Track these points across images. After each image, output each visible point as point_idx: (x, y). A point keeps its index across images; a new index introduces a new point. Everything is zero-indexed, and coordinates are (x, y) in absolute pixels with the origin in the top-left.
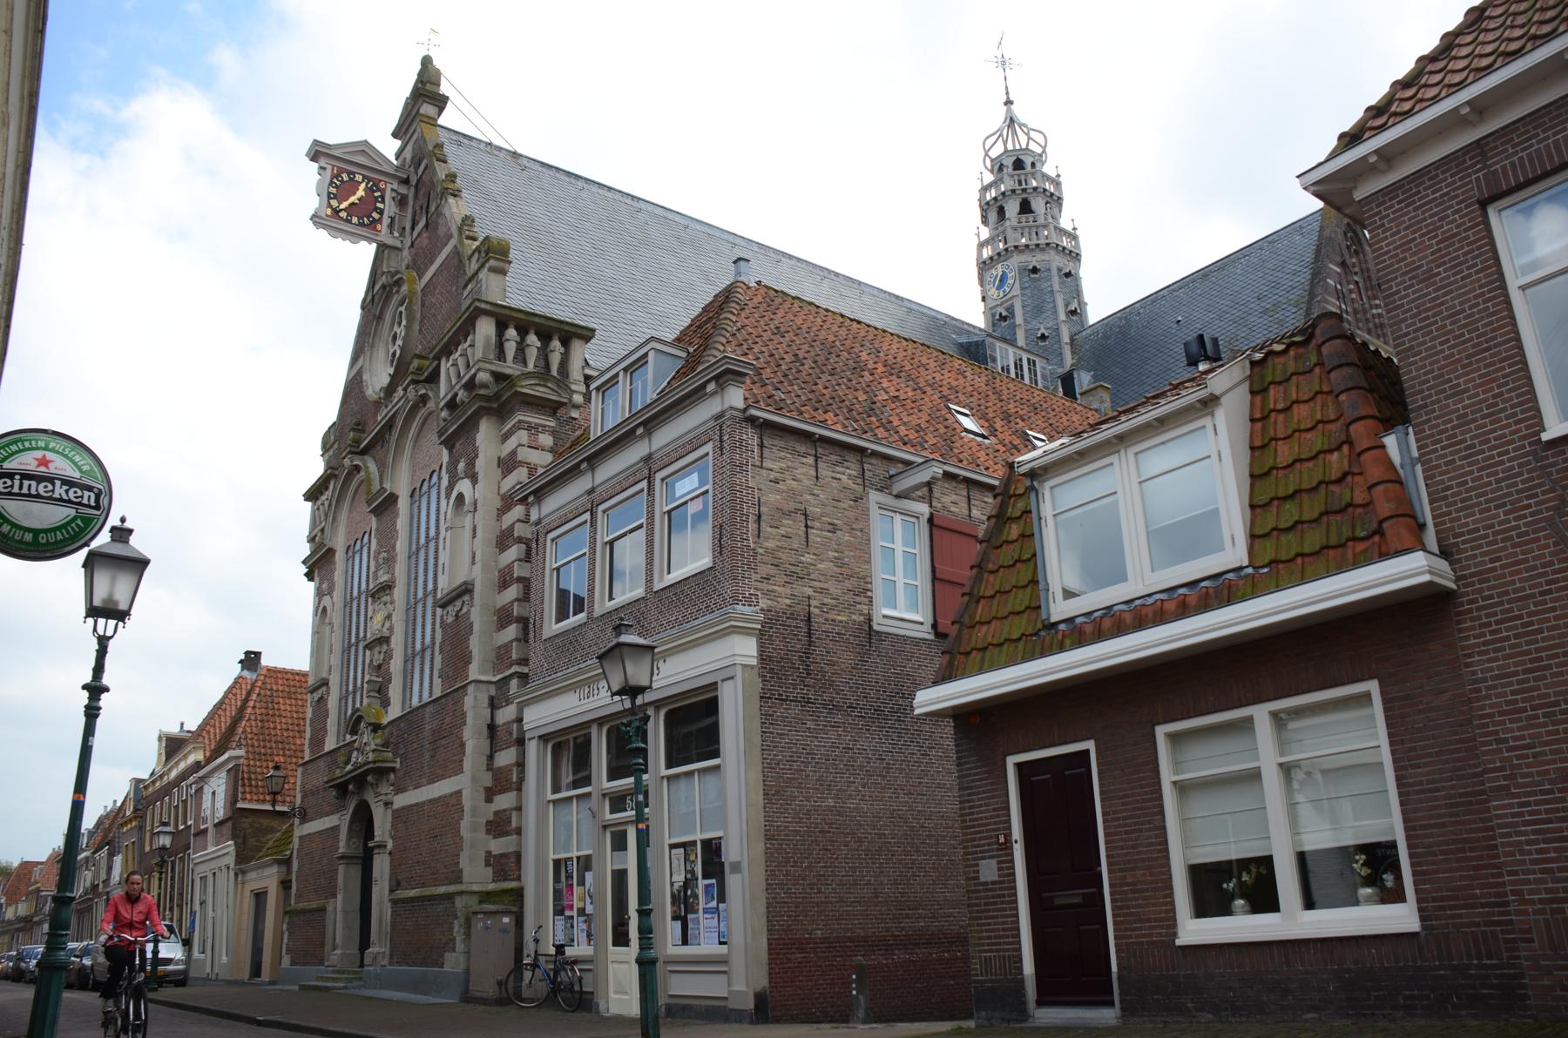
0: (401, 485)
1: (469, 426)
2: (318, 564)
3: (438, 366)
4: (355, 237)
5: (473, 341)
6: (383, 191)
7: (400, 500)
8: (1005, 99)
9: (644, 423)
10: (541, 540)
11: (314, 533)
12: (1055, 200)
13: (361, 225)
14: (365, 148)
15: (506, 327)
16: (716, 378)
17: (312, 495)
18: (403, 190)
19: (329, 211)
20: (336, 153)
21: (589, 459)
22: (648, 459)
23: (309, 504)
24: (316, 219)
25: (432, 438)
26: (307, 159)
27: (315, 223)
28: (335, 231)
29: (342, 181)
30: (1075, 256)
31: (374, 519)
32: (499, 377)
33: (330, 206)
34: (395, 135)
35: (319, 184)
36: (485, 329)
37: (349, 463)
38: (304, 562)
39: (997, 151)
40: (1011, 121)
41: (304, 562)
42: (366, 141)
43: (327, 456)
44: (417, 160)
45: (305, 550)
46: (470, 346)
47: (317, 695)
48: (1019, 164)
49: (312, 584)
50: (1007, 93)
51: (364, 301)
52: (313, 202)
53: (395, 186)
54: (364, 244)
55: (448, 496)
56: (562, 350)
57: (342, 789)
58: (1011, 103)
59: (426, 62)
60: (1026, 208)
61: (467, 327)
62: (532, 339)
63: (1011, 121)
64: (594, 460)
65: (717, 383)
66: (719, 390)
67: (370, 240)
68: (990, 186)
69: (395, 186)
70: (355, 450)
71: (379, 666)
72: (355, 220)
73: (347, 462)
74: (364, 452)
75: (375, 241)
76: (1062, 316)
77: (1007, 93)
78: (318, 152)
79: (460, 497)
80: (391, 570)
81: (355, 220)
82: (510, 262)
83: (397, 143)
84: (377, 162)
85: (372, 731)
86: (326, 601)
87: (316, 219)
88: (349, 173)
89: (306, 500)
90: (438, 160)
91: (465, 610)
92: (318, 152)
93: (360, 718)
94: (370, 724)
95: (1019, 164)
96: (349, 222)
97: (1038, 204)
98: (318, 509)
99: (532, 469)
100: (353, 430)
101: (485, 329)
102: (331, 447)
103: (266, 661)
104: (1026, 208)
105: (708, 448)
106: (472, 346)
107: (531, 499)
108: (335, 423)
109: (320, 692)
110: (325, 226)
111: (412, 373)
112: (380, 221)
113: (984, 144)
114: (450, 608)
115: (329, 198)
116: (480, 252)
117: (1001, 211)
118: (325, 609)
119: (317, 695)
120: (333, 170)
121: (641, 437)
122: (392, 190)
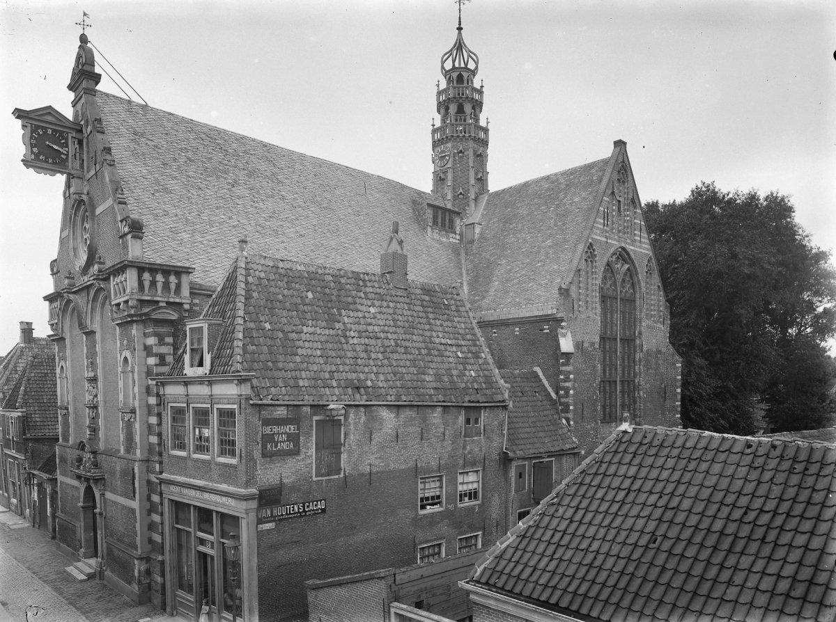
0: (96, 327)
4: (53, 172)
6: (67, 139)
8: (458, 26)
12: (477, 105)
13: (54, 163)
14: (49, 110)
15: (144, 272)
18: (79, 136)
19: (33, 157)
20: (32, 116)
26: (13, 117)
28: (39, 169)
29: (39, 134)
30: (485, 143)
31: (84, 337)
33: (32, 152)
39: (448, 65)
40: (460, 46)
42: (50, 106)
48: (460, 78)
50: (460, 22)
52: (21, 150)
53: (74, 135)
54: (58, 175)
56: (176, 281)
58: (462, 29)
59: (84, 39)
60: (461, 110)
62: (160, 278)
63: (460, 46)
67: (62, 173)
68: (445, 91)
69: (74, 135)
72: (50, 161)
75: (65, 173)
76: (472, 181)
77: (460, 22)
78: (19, 114)
81: (50, 161)
87: (27, 163)
88: (43, 128)
90: (98, 132)
92: (19, 114)
95: (460, 78)
96: (48, 162)
97: (468, 108)
100: (68, 278)
103: (36, 334)
104: (461, 110)
110: (32, 166)
112: (67, 159)
113: (442, 58)
115: (32, 147)
117: (447, 108)
120: (31, 127)
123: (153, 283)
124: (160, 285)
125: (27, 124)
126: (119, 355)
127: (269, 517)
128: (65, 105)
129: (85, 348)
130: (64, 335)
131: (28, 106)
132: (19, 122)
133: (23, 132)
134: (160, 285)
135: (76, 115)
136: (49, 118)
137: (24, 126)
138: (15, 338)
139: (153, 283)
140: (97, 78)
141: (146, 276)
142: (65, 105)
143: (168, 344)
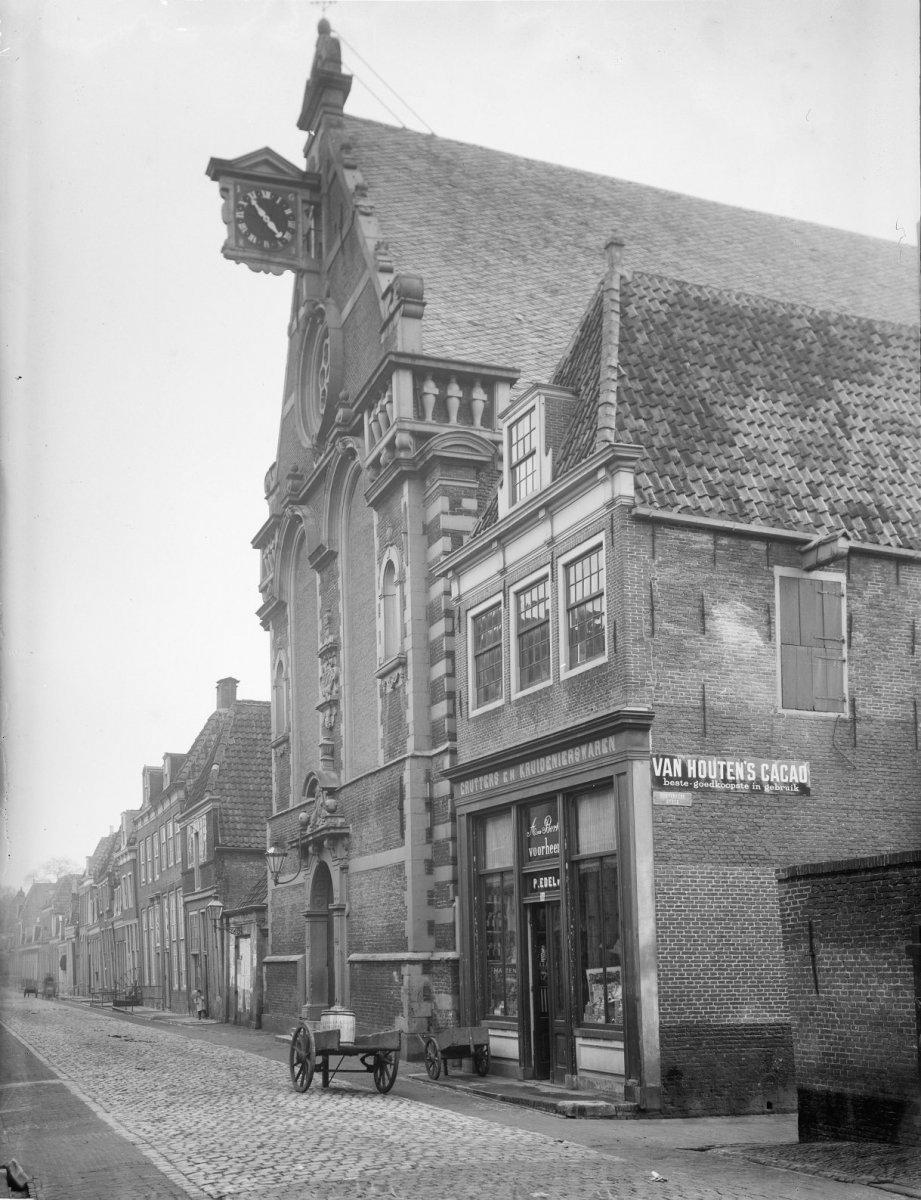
1: (394, 488)
2: (272, 614)
3: (362, 419)
5: (391, 397)
7: (339, 559)
9: (546, 506)
10: (463, 619)
11: (264, 584)
14: (267, 157)
16: (606, 465)
17: (260, 542)
21: (498, 538)
22: (551, 542)
23: (258, 551)
24: (229, 252)
25: (361, 503)
26: (208, 178)
27: (227, 257)
32: (421, 437)
34: (303, 124)
35: (225, 209)
36: (402, 384)
37: (290, 514)
38: (259, 613)
41: (259, 613)
42: (267, 151)
43: (273, 497)
44: (327, 161)
45: (258, 601)
46: (388, 402)
47: (280, 750)
49: (268, 633)
51: (290, 327)
52: (221, 233)
55: (380, 564)
56: (485, 397)
57: (304, 854)
59: (324, 28)
61: (380, 386)
62: (455, 390)
64: (503, 540)
65: (607, 470)
66: (608, 476)
70: (295, 499)
71: (331, 729)
73: (288, 512)
74: (304, 501)
78: (218, 169)
79: (390, 565)
80: (333, 630)
82: (424, 304)
83: (304, 136)
84: (285, 173)
85: (327, 795)
86: (282, 655)
87: (229, 252)
89: (254, 548)
91: (400, 683)
92: (218, 169)
93: (315, 782)
94: (324, 789)
98: (267, 557)
99: (457, 537)
100: (289, 477)
101: (402, 384)
102: (274, 491)
103: (241, 694)
105: (601, 537)
106: (390, 402)
107: (450, 575)
108: (275, 463)
109: (282, 747)
111: (338, 425)
114: (387, 679)
116: (392, 291)
118: (280, 663)
119: (280, 750)
120: (236, 190)
121: (544, 520)
122: (304, 202)
123: (442, 403)
124: (454, 405)
125: (227, 186)
126: (377, 566)
127: (677, 779)
128: (293, 147)
129: (319, 598)
130: (284, 598)
131: (230, 153)
132: (216, 186)
133: (222, 201)
134: (454, 405)
135: (311, 164)
136: (264, 171)
137: (224, 191)
138: (208, 705)
139: (442, 403)
140: (343, 85)
141: (431, 388)
142: (293, 147)
143: (468, 513)
